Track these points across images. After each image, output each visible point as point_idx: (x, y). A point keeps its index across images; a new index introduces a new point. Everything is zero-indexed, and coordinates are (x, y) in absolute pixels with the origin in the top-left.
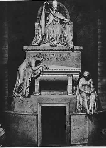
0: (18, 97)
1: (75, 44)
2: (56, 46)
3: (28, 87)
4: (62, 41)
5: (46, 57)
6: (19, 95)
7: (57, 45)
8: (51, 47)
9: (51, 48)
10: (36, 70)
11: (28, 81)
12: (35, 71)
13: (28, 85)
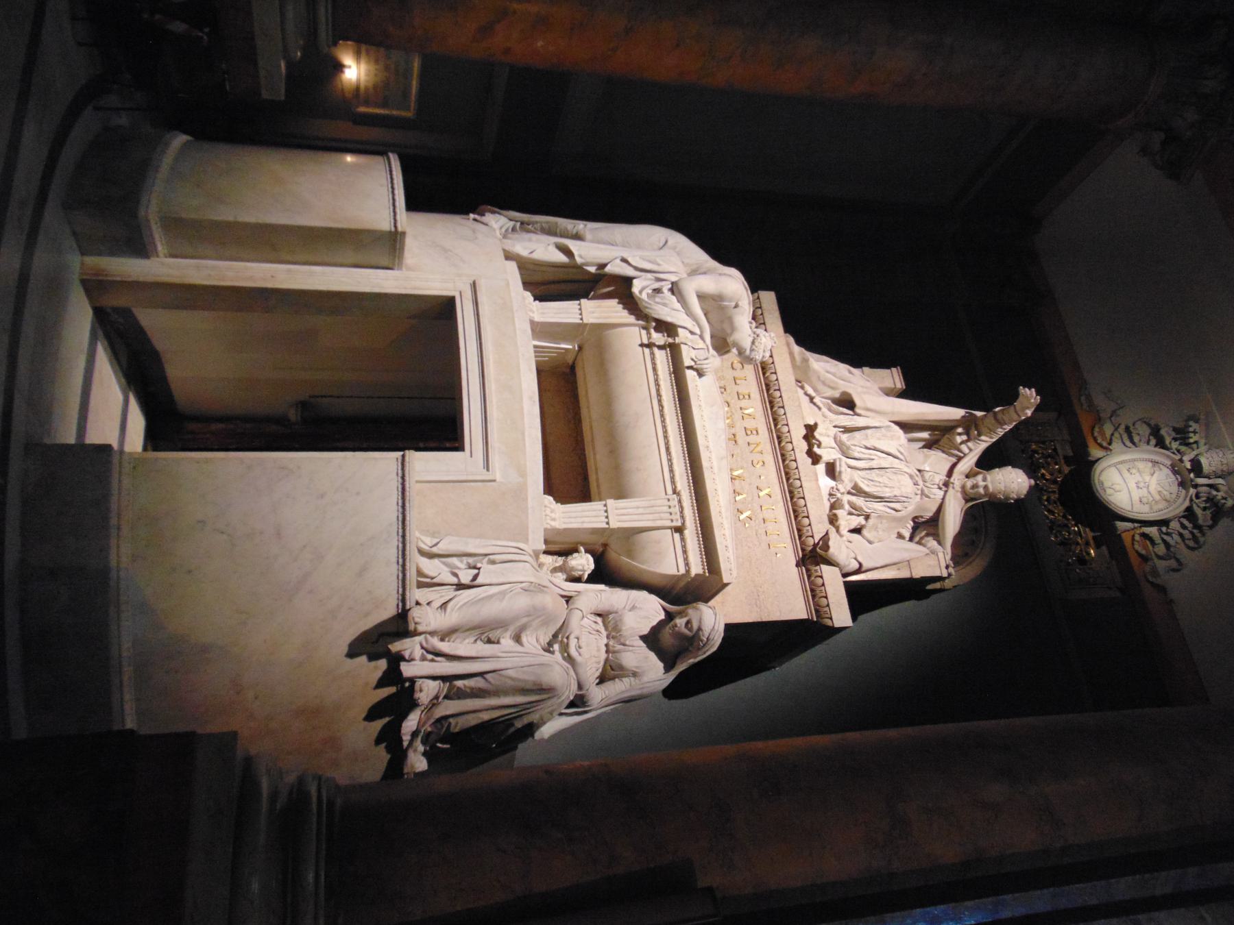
2: (816, 459)
7: (821, 468)
8: (804, 432)
12: (675, 289)
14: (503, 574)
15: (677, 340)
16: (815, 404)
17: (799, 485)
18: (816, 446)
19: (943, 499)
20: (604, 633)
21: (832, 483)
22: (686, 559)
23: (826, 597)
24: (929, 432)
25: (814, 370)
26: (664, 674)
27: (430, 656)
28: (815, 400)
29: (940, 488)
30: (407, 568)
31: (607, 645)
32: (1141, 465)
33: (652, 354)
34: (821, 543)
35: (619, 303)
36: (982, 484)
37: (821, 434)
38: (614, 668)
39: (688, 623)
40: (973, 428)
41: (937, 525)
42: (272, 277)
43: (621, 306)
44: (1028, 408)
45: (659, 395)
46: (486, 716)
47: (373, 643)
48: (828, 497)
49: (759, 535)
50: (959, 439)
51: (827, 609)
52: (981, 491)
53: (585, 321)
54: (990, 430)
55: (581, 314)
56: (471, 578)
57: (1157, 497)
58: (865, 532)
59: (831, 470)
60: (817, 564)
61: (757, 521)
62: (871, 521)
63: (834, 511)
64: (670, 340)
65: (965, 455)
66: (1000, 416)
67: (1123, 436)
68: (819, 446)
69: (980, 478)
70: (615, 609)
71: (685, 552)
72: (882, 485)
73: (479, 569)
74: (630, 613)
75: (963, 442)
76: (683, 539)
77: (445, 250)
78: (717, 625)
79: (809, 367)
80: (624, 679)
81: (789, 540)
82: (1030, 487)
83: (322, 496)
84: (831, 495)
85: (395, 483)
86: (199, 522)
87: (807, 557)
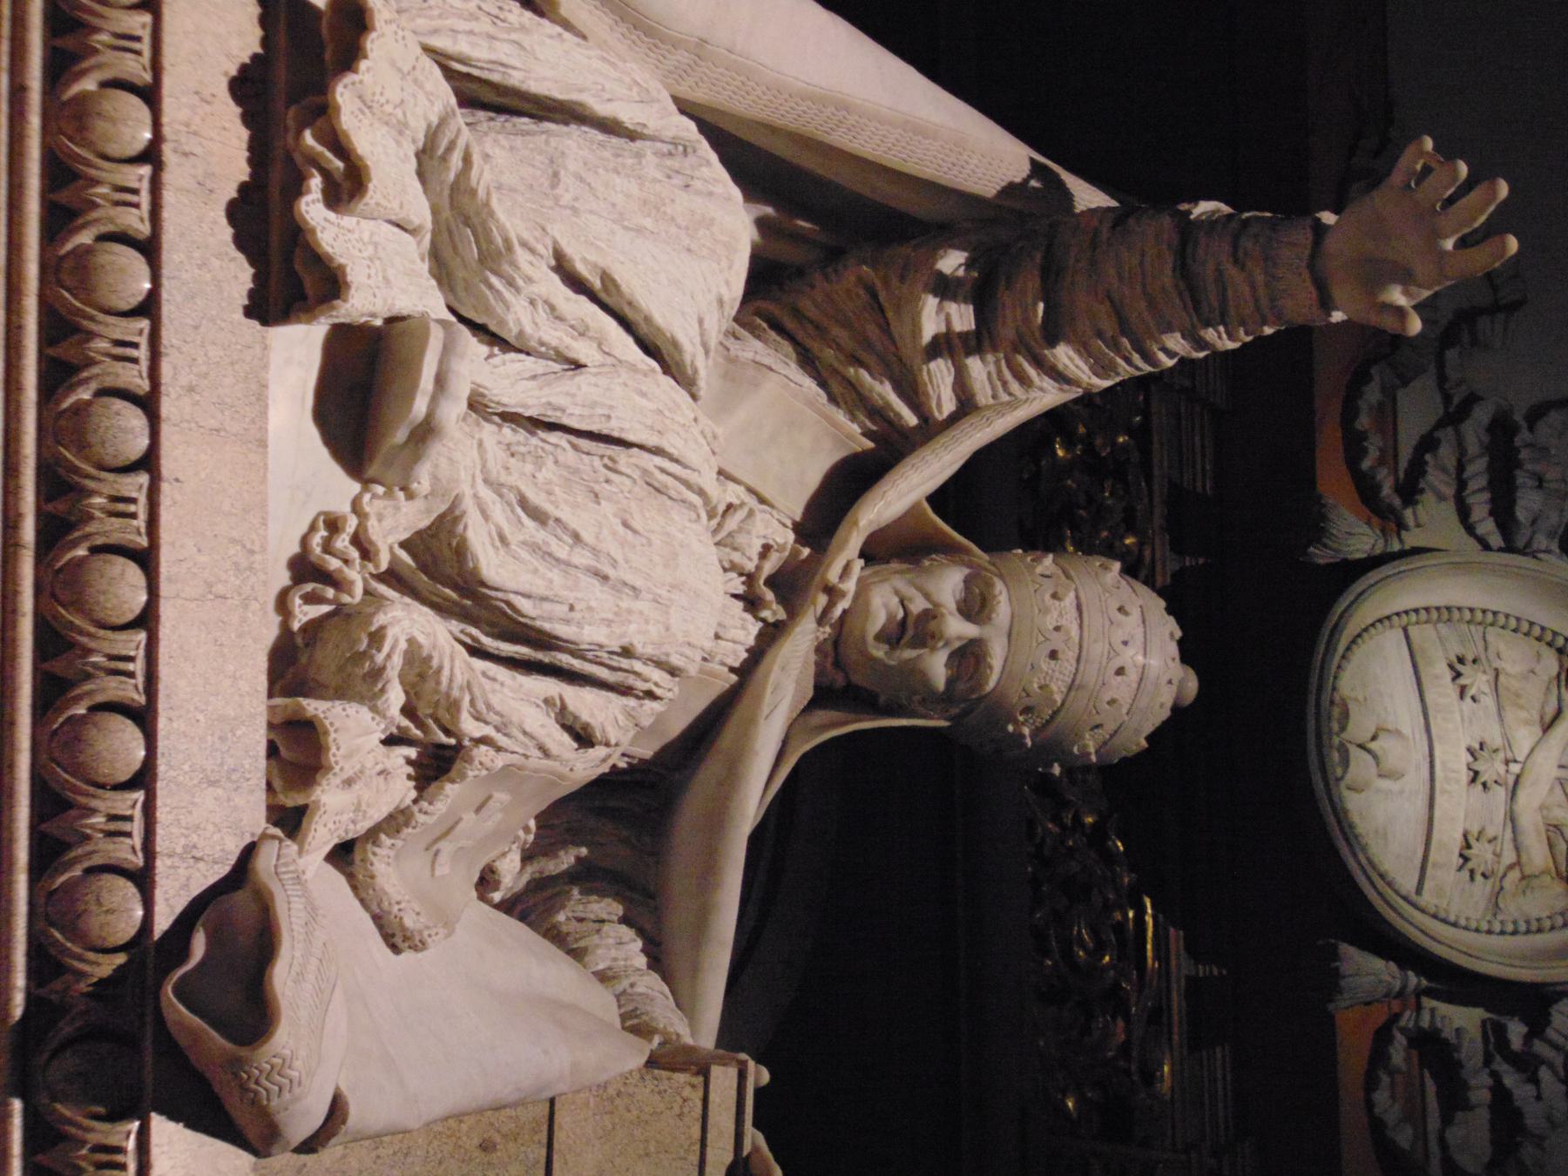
18: (316, 182)
24: (769, 210)
32: (1513, 656)
34: (199, 945)
37: (366, 104)
44: (1406, 278)
48: (283, 578)
52: (937, 667)
54: (1124, 327)
57: (1538, 855)
65: (930, 430)
66: (1212, 257)
67: (1471, 469)
69: (948, 583)
75: (943, 345)
84: (304, 569)
87: (66, 1029)
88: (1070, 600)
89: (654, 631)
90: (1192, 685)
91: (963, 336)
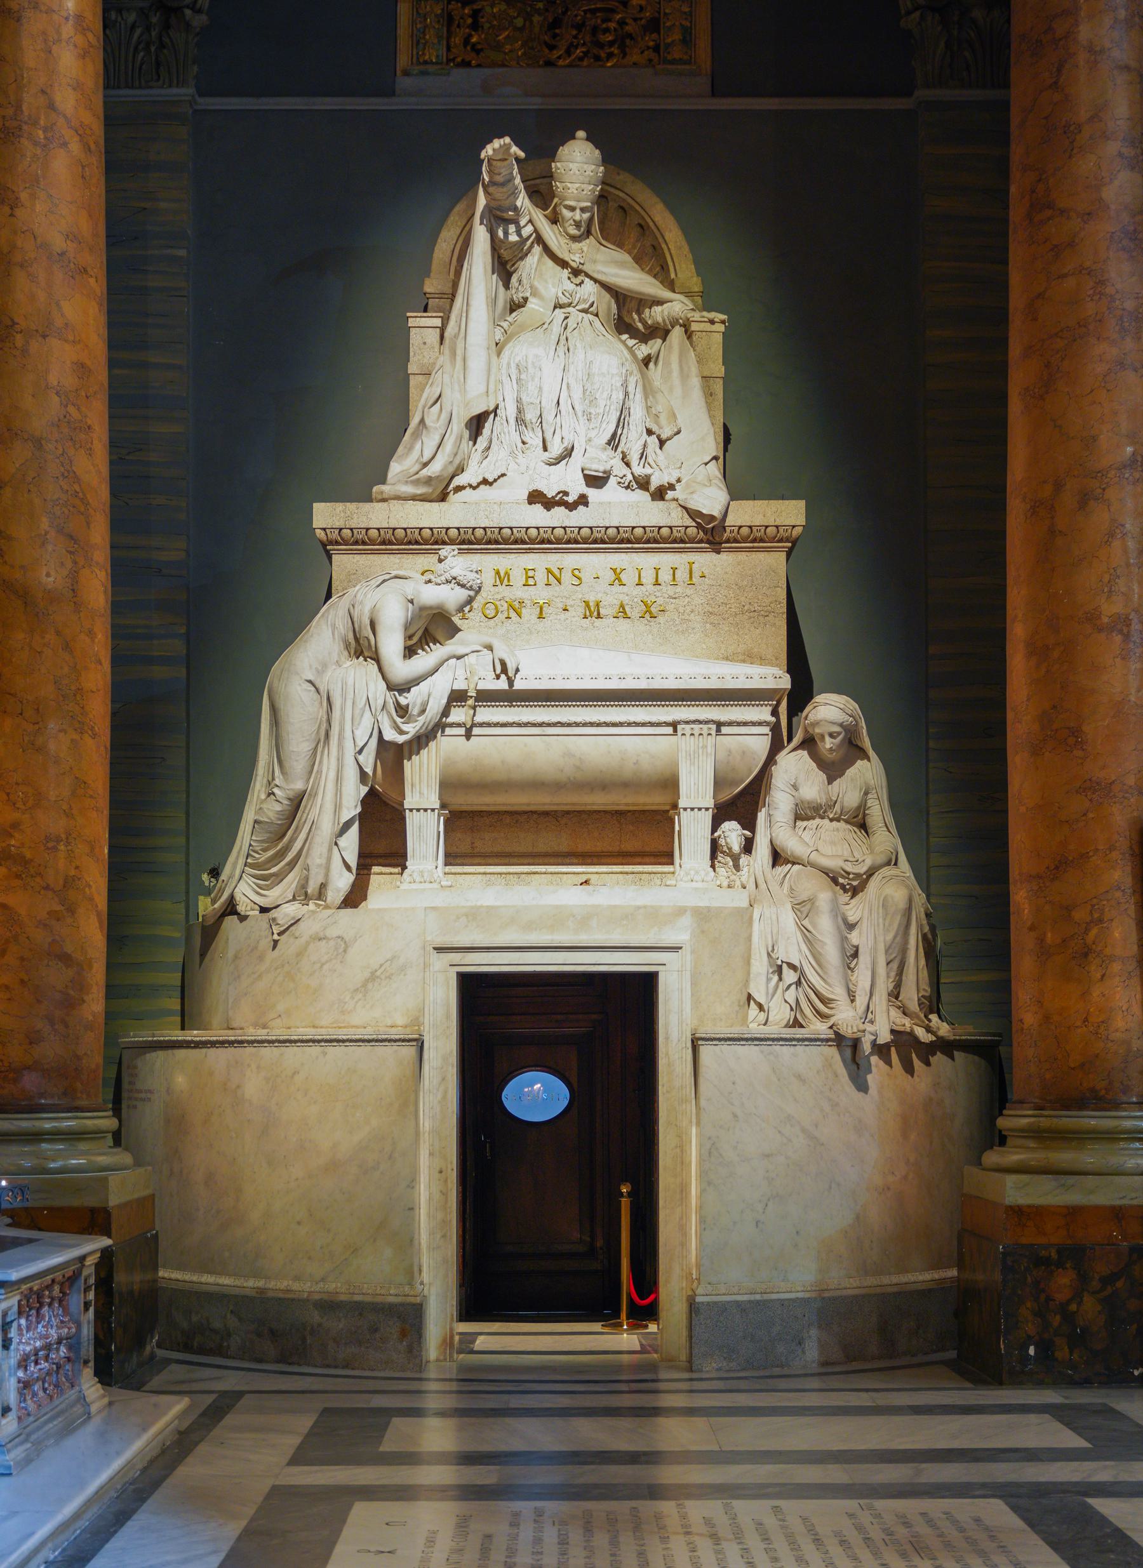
0: (264, 910)
1: (737, 492)
2: (583, 500)
3: (347, 826)
4: (634, 458)
5: (503, 590)
6: (273, 895)
7: (592, 494)
8: (538, 507)
9: (538, 517)
10: (417, 681)
11: (351, 775)
12: (404, 688)
13: (351, 809)
14: (788, 938)
15: (472, 693)
16: (495, 480)
17: (615, 530)
18: (565, 498)
19: (596, 281)
20: (818, 821)
21: (612, 481)
22: (753, 724)
23: (767, 527)
25: (442, 470)
26: (869, 760)
27: (870, 1016)
28: (491, 480)
29: (582, 282)
30: (801, 1036)
31: (831, 820)
33: (481, 725)
35: (410, 759)
36: (577, 216)
38: (855, 815)
39: (831, 735)
40: (505, 215)
41: (625, 296)
42: (441, 1172)
43: (414, 757)
45: (541, 725)
46: (922, 962)
47: (858, 1068)
49: (677, 595)
50: (513, 238)
51: (781, 529)
52: (586, 216)
53: (437, 806)
55: (426, 810)
56: (792, 972)
58: (664, 436)
59: (596, 481)
60: (724, 528)
61: (658, 594)
62: (655, 428)
63: (652, 488)
64: (471, 702)
65: (536, 231)
68: (566, 494)
69: (567, 213)
70: (794, 806)
71: (745, 724)
72: (608, 404)
73: (782, 962)
74: (801, 790)
76: (730, 724)
77: (373, 977)
78: (838, 705)
79: (438, 477)
80: (869, 805)
81: (683, 555)
82: (588, 139)
83: (735, 1116)
84: (627, 488)
85: (725, 1049)
86: (757, 1226)
87: (711, 539)
88: (569, 185)
89: (618, 378)
90: (581, 134)
91: (516, 227)
